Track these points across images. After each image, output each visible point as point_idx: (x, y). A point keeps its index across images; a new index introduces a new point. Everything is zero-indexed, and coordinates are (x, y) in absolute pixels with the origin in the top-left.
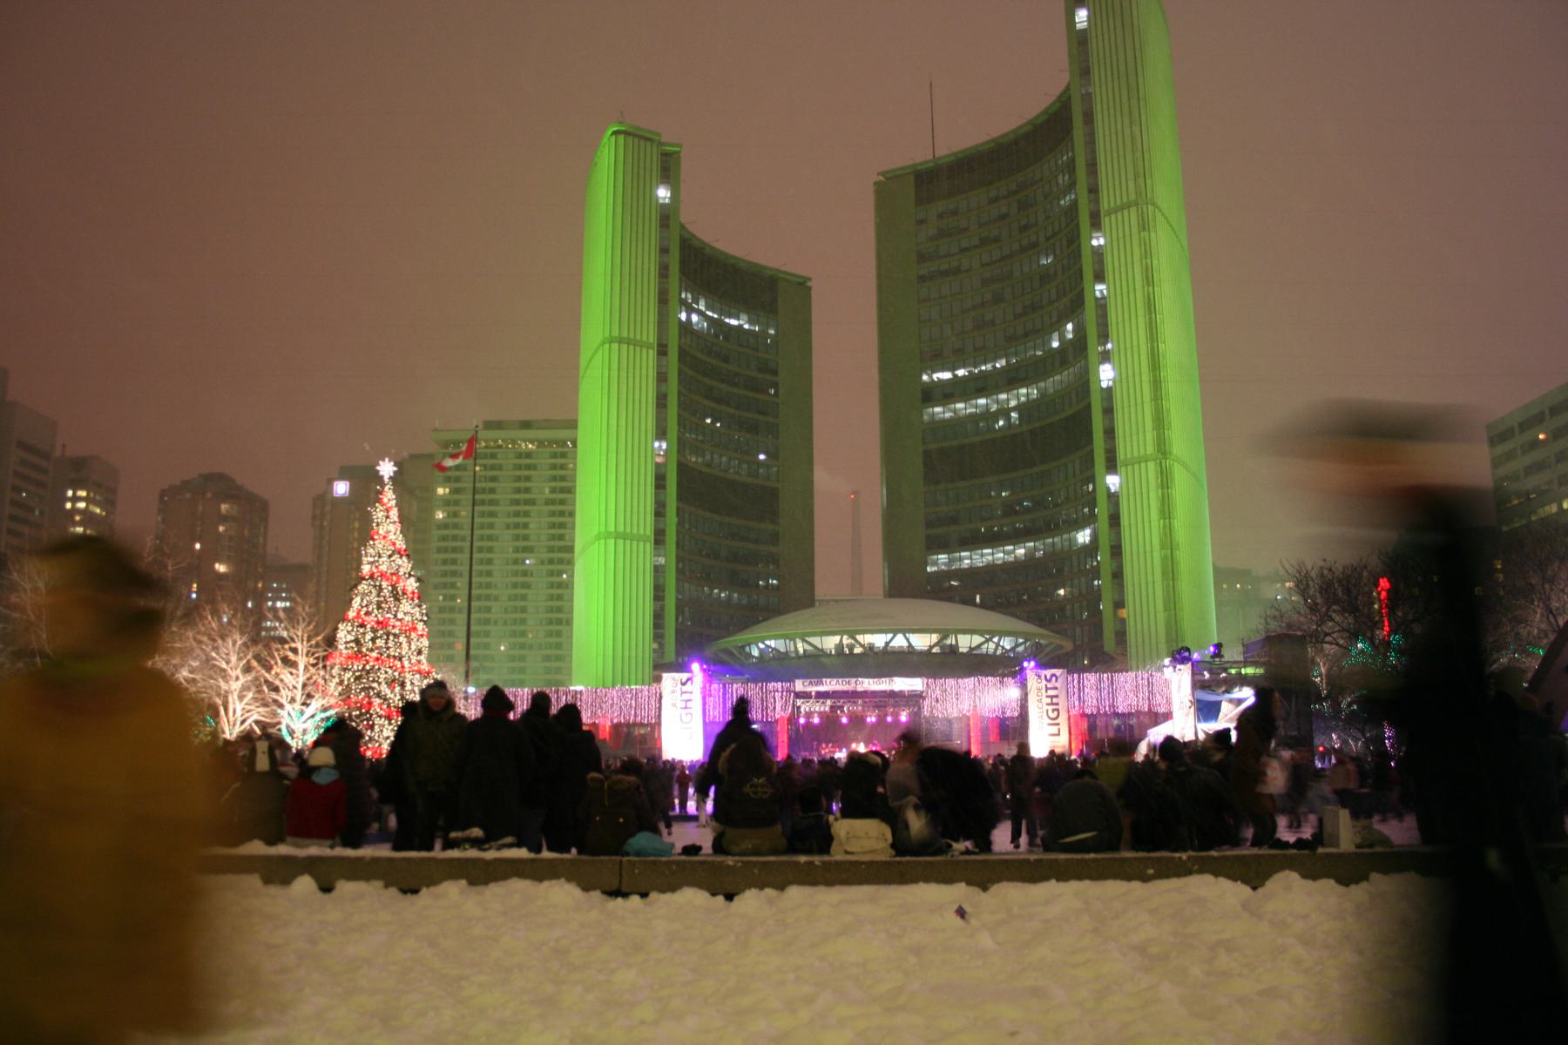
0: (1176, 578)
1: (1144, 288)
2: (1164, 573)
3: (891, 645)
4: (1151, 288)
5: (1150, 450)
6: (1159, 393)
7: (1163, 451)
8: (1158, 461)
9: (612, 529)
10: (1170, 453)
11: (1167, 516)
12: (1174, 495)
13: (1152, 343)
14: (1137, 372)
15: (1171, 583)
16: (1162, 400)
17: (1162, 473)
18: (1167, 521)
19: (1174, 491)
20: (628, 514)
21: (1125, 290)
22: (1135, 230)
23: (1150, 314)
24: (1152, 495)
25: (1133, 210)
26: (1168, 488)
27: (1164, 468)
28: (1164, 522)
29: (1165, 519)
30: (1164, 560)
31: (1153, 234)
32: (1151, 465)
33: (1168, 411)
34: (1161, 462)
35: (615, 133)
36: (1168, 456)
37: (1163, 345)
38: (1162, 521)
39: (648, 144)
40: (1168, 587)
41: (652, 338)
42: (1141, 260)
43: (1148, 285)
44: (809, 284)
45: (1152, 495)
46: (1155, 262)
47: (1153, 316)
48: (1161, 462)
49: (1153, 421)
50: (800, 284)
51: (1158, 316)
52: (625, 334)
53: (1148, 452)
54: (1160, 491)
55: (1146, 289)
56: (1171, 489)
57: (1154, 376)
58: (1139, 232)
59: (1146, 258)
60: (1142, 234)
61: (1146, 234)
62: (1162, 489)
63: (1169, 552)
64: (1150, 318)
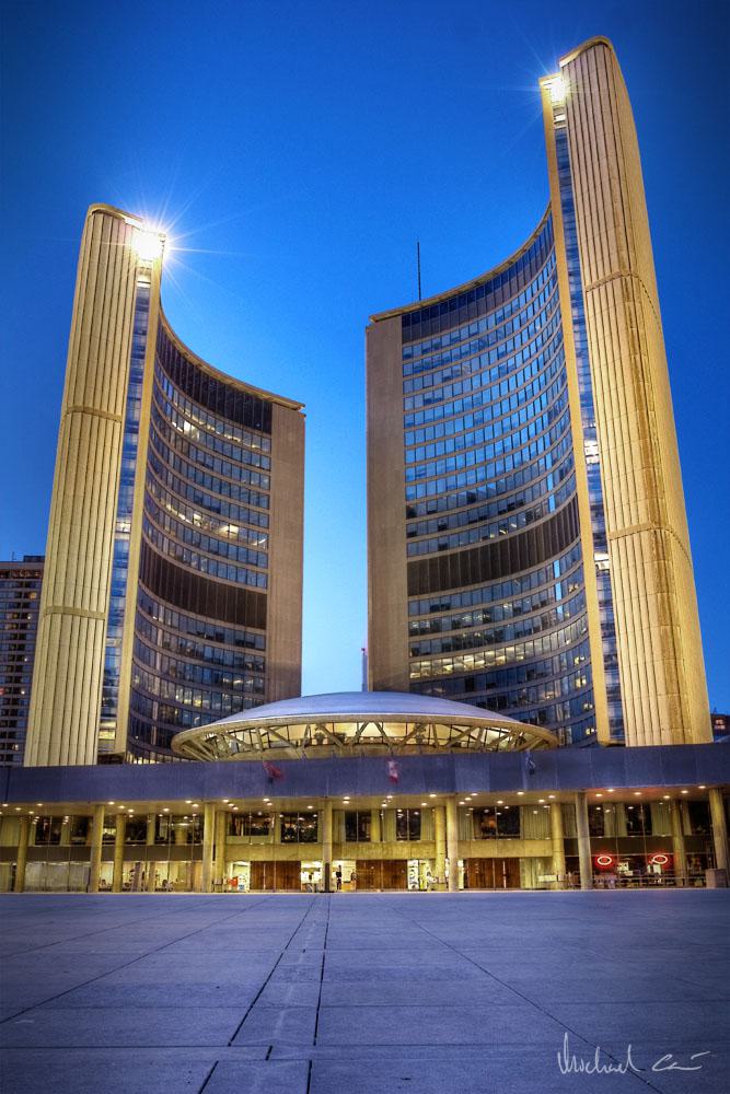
2: (663, 651)
3: (363, 734)
5: (644, 519)
7: (657, 520)
11: (665, 588)
13: (641, 409)
15: (672, 661)
17: (657, 542)
22: (619, 301)
27: (659, 537)
28: (662, 598)
30: (663, 638)
32: (645, 535)
35: (94, 212)
36: (663, 526)
38: (659, 595)
40: (669, 668)
43: (635, 353)
44: (302, 410)
50: (295, 409)
62: (658, 560)
63: (668, 628)
64: (639, 386)
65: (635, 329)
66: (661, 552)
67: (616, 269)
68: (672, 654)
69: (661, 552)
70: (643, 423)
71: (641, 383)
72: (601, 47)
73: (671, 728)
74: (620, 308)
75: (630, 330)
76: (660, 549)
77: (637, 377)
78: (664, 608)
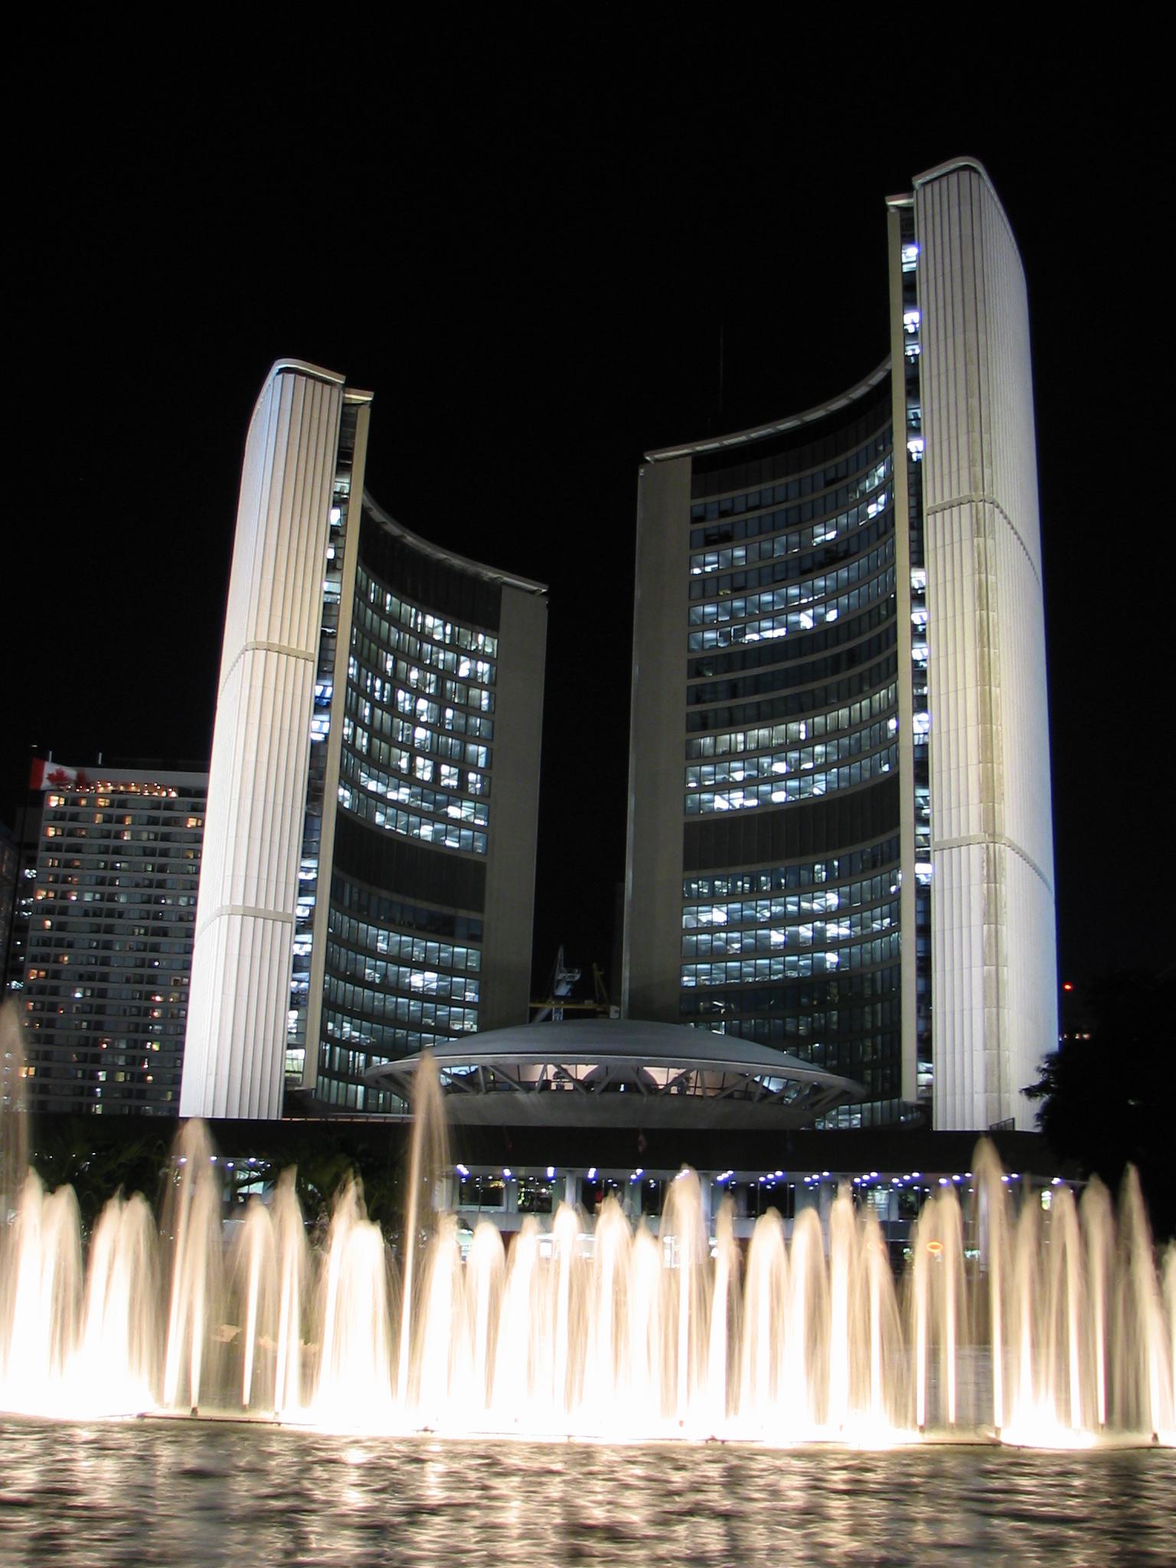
0: (1001, 1004)
1: (975, 611)
2: (985, 998)
4: (984, 613)
5: (975, 829)
6: (989, 753)
7: (991, 831)
8: (984, 845)
9: (239, 902)
10: (1001, 836)
11: (993, 919)
12: (1004, 892)
13: (983, 685)
14: (961, 725)
15: (994, 1010)
16: (992, 762)
18: (993, 926)
19: (1003, 887)
20: (264, 883)
21: (950, 614)
23: (982, 647)
24: (975, 890)
25: (965, 508)
26: (996, 882)
28: (989, 930)
29: (989, 924)
30: (985, 979)
31: (990, 542)
33: (1001, 777)
34: (988, 847)
35: (281, 371)
37: (998, 689)
38: (985, 926)
39: (327, 388)
41: (313, 648)
42: (973, 574)
43: (981, 610)
45: (975, 890)
46: (991, 578)
47: (986, 649)
48: (988, 847)
49: (981, 791)
51: (992, 651)
52: (276, 640)
53: (971, 834)
54: (985, 885)
55: (978, 612)
56: (1001, 884)
57: (984, 730)
58: (972, 538)
59: (979, 573)
60: (975, 540)
61: (982, 540)
62: (988, 883)
65: (983, 576)
66: (992, 872)
67: (965, 492)
68: (995, 1001)
69: (992, 872)
70: (983, 702)
71: (986, 649)
72: (965, 175)
73: (986, 1091)
74: (966, 544)
75: (977, 576)
76: (992, 868)
77: (981, 641)
78: (990, 945)
